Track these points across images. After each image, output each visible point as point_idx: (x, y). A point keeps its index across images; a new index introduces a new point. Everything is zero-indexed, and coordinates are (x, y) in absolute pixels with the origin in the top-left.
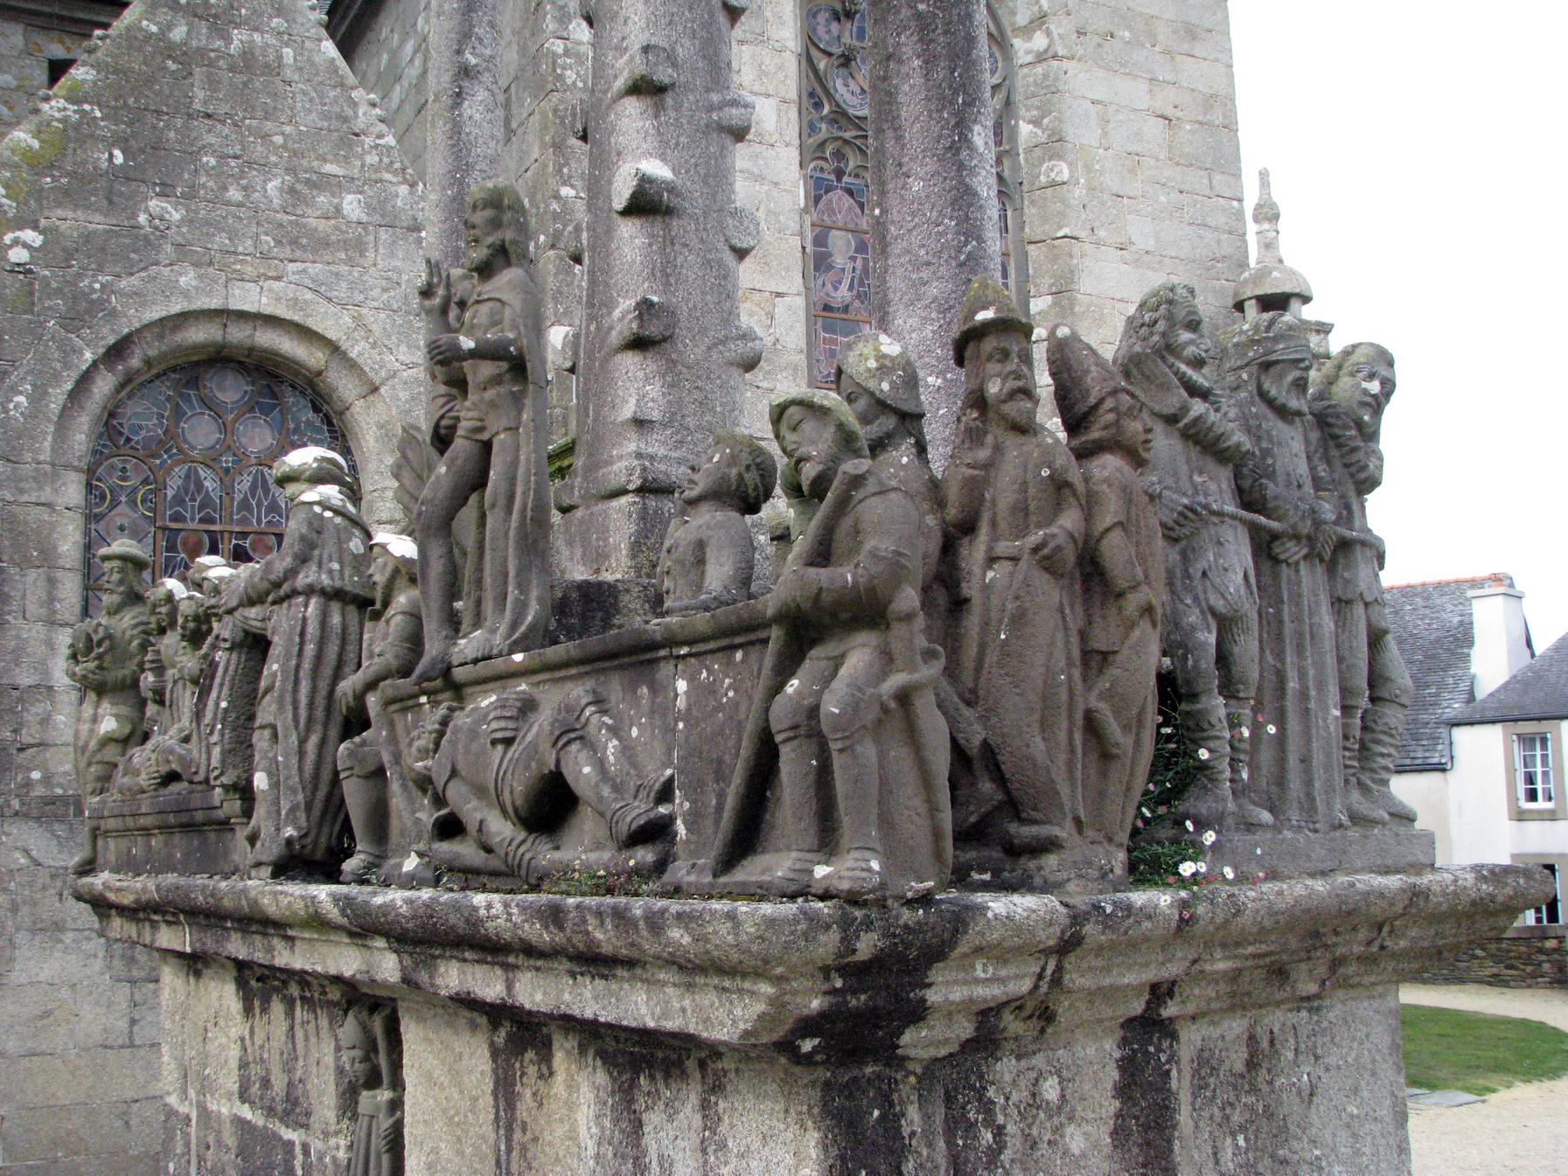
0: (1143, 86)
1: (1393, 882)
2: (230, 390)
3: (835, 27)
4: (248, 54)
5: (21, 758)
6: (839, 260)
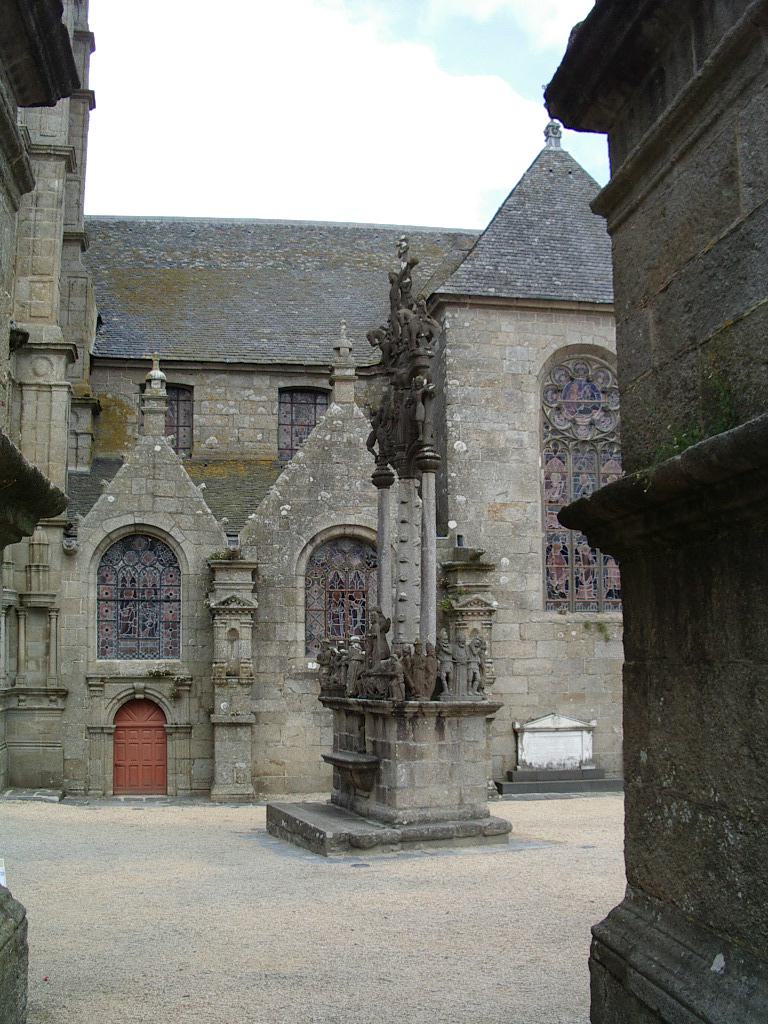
1: (470, 702)
2: (347, 547)
3: (555, 396)
4: (349, 442)
5: (289, 662)
6: (555, 484)
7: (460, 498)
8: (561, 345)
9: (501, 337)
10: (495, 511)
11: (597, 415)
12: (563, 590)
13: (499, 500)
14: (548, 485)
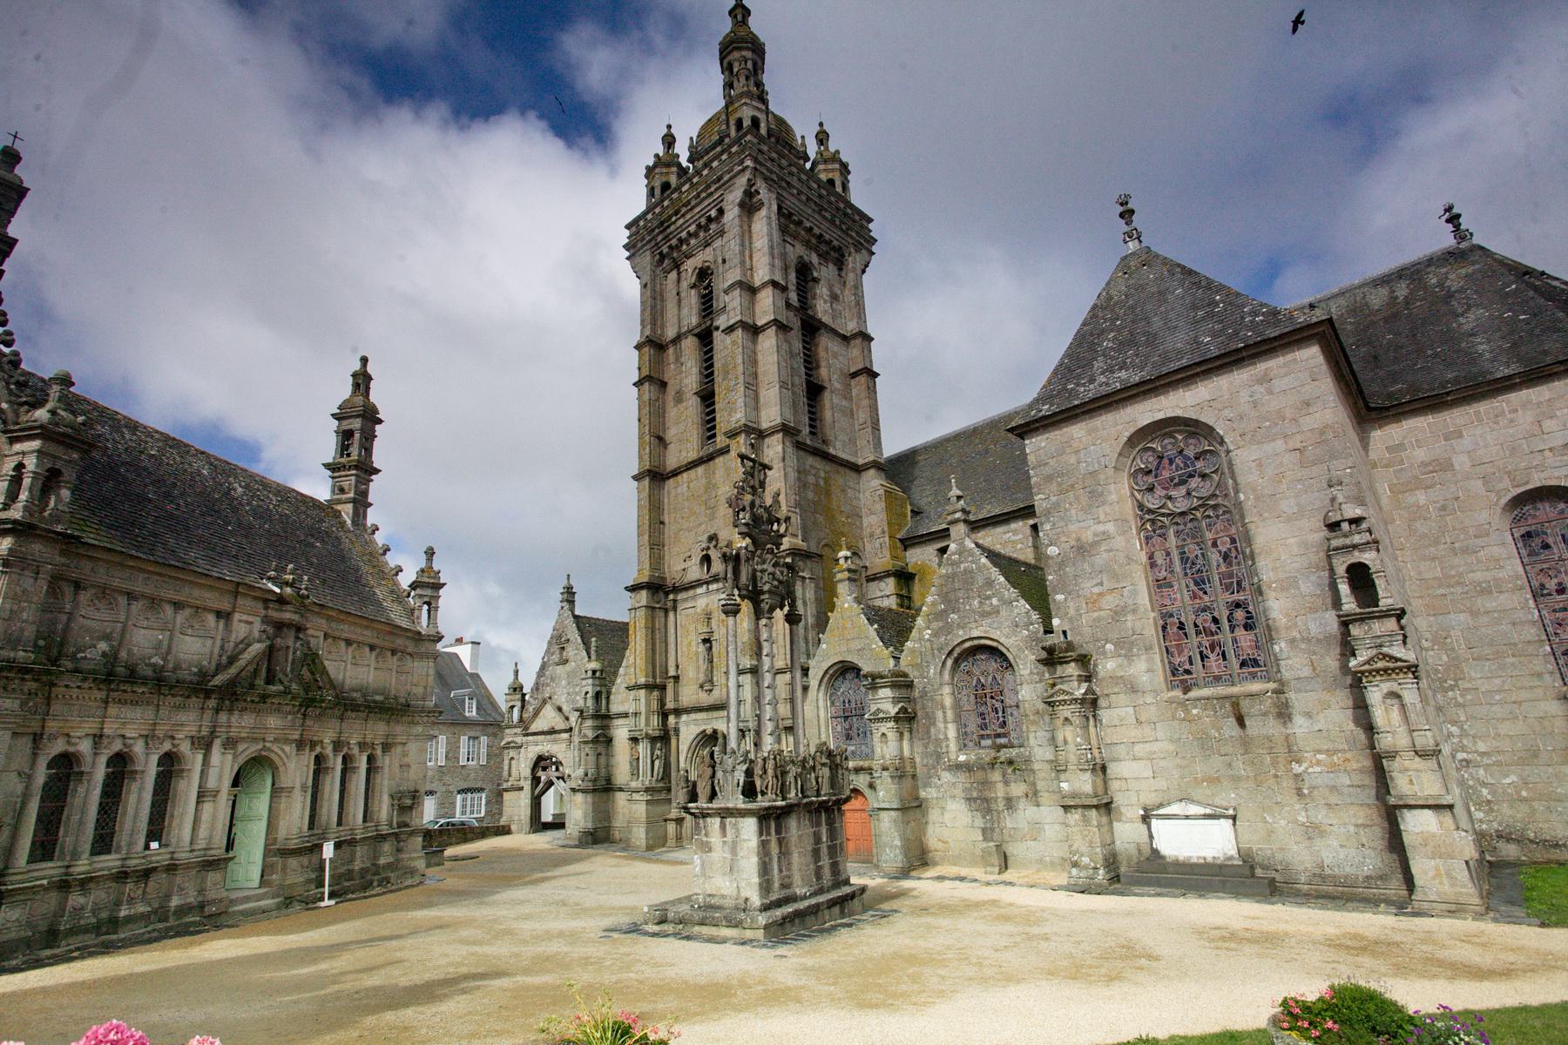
0: (1280, 442)
6: (1159, 562)
7: (1060, 597)
8: (1133, 430)
9: (1075, 444)
10: (1093, 603)
11: (1194, 483)
12: (1187, 666)
13: (1096, 590)
14: (1153, 565)
